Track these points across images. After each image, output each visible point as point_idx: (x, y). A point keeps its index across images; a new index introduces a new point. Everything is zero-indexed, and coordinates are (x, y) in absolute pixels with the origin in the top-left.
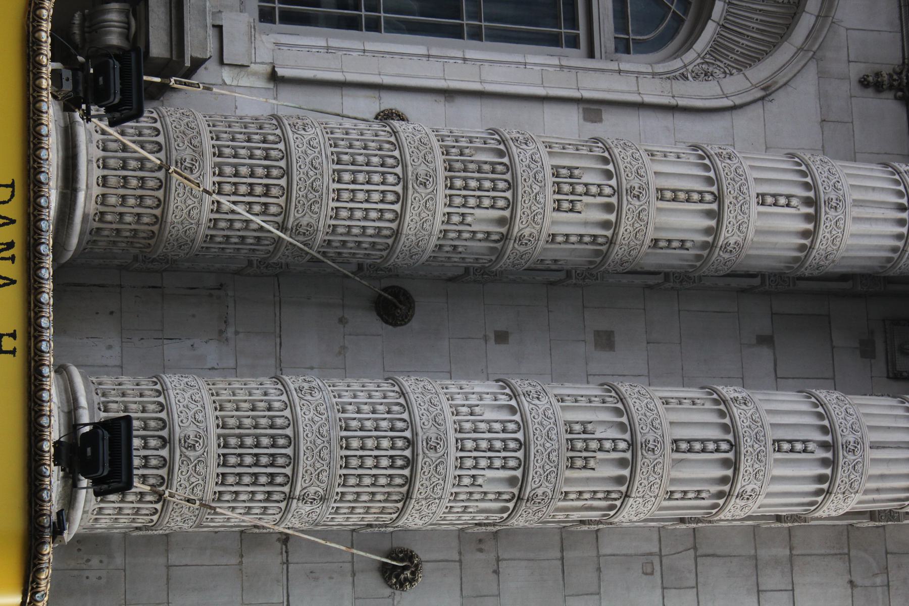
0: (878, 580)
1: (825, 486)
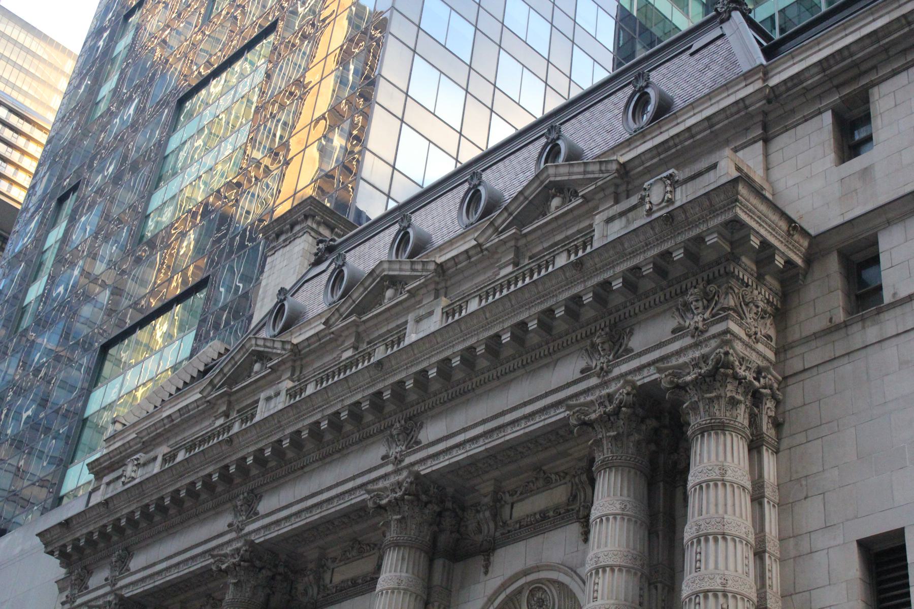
0: (804, 483)
1: (720, 537)
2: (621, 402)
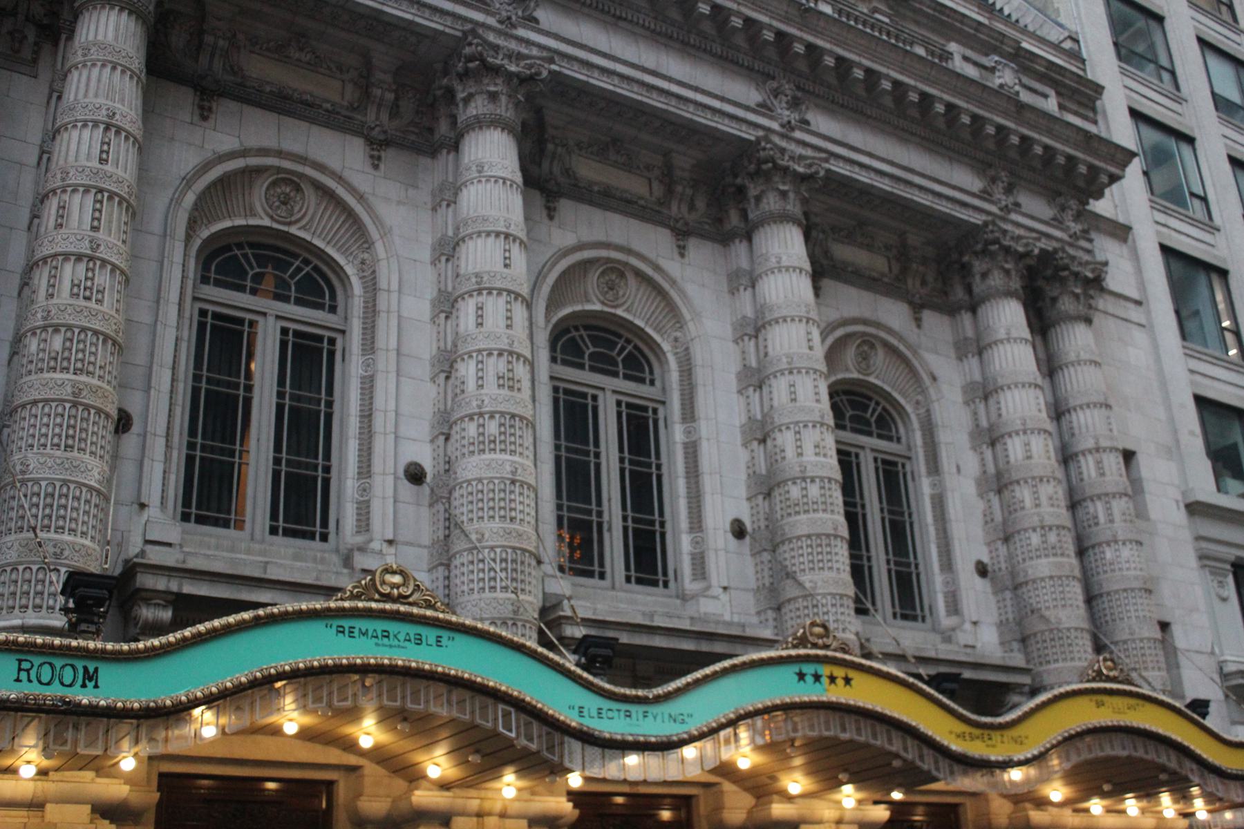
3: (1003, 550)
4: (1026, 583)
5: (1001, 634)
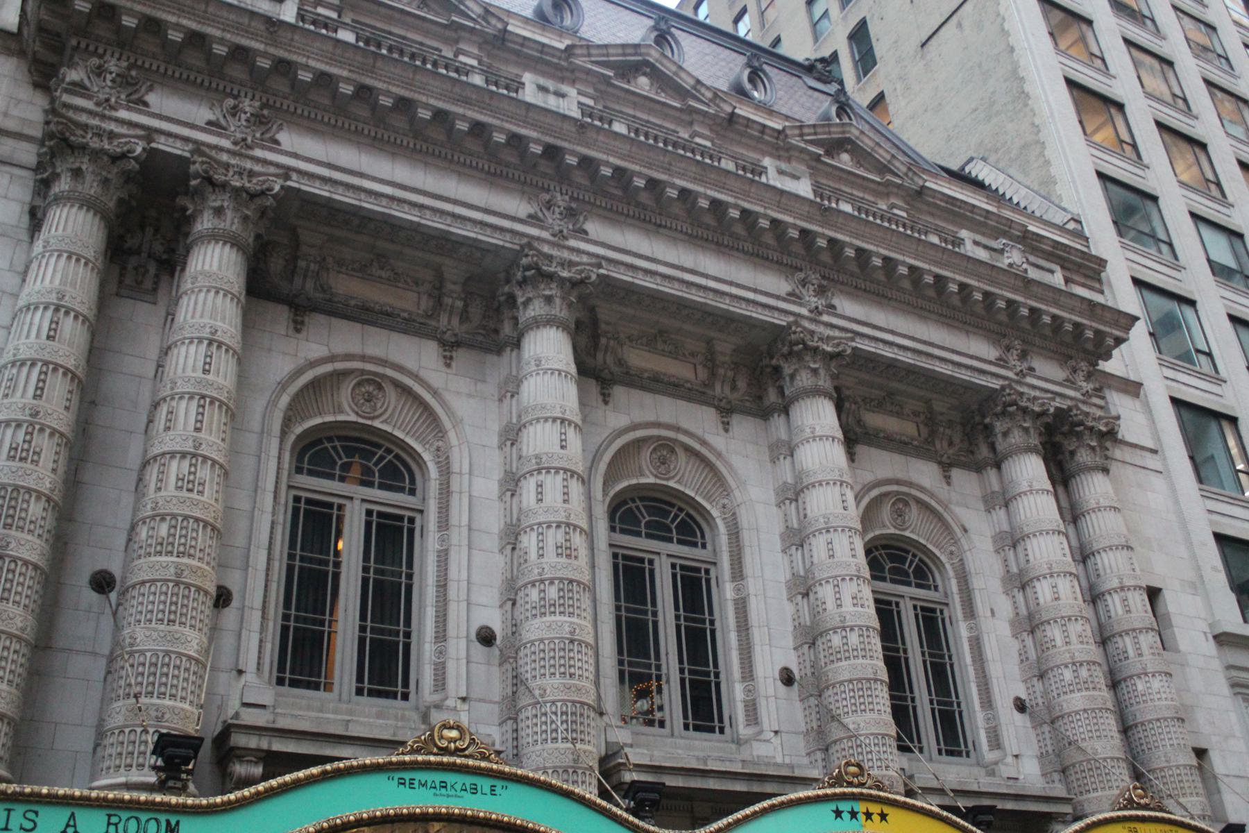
2: (129, 152)
3: (1039, 686)
4: (1062, 717)
5: (1042, 766)
